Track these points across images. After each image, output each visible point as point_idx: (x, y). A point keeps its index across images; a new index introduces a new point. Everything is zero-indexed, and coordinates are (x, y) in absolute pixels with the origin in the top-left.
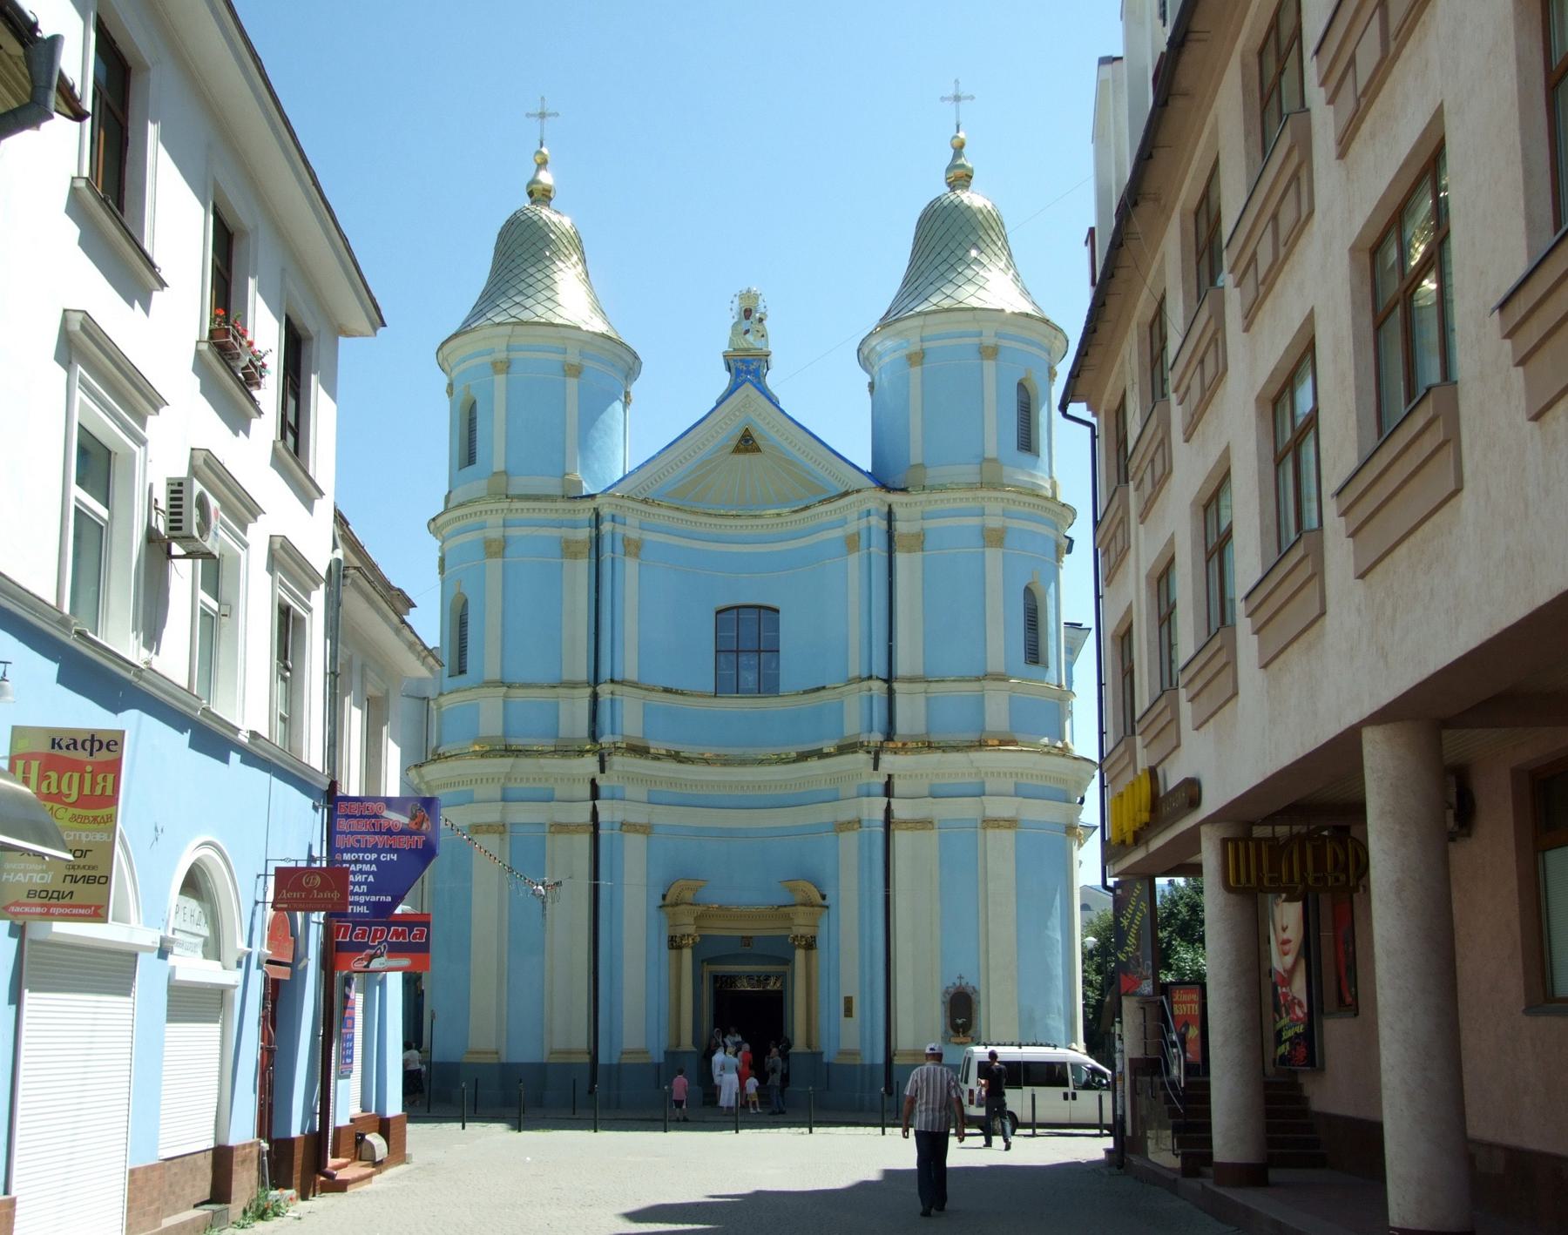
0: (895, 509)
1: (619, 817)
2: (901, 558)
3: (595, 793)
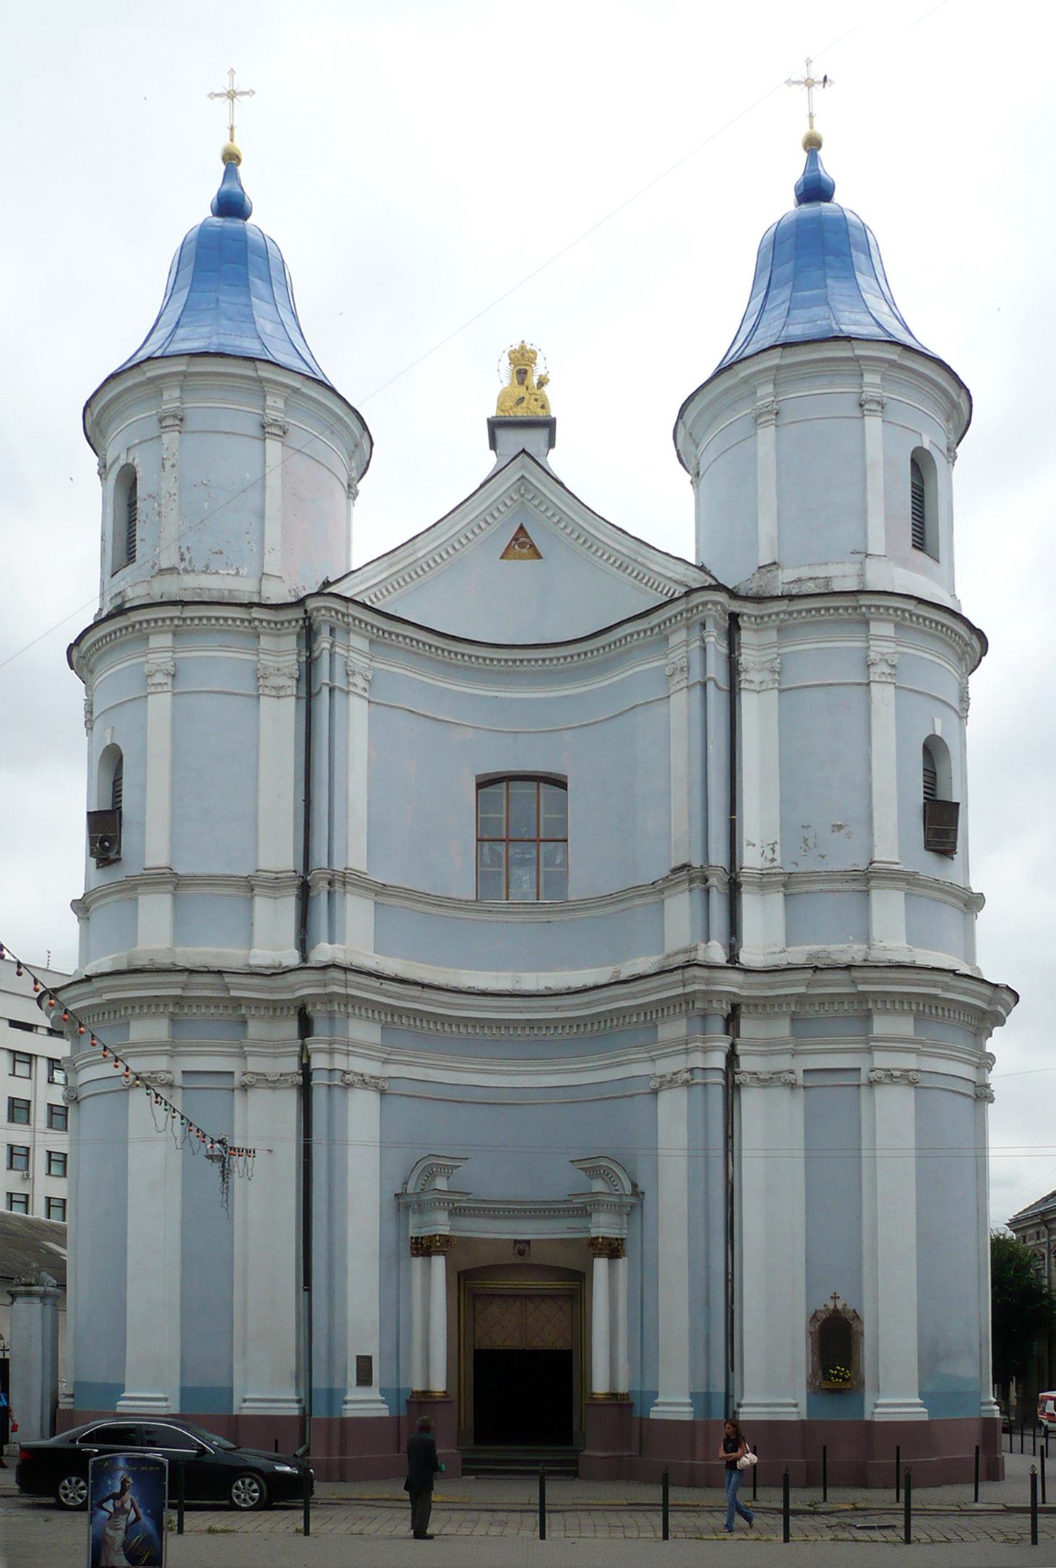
1: (340, 1062)
2: (749, 704)
3: (306, 1027)
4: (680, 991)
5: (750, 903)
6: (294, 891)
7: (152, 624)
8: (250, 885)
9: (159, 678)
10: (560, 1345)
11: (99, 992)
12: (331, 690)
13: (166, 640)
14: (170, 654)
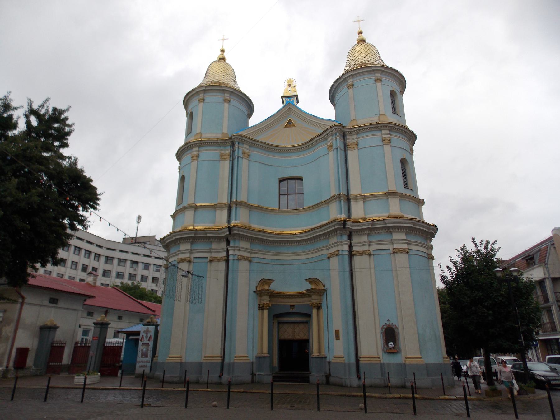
2: (349, 153)
3: (228, 243)
4: (334, 228)
5: (353, 203)
9: (195, 158)
10: (305, 338)
11: (172, 237)
12: (238, 158)
13: (197, 149)
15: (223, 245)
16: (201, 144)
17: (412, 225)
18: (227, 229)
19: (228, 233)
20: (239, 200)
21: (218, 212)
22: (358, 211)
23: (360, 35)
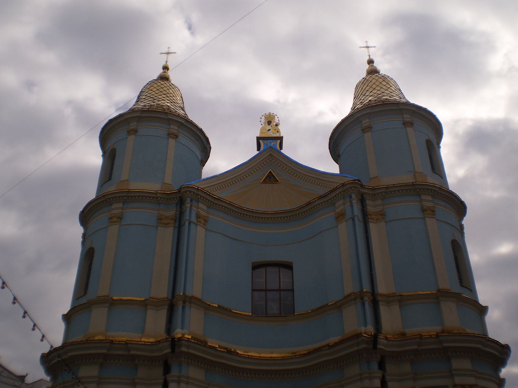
0: (365, 196)
2: (372, 226)
4: (355, 348)
5: (383, 310)
6: (167, 307)
7: (115, 199)
8: (145, 304)
9: (115, 219)
13: (120, 205)
14: (121, 210)
15: (158, 372)
16: (129, 197)
17: (480, 346)
18: (168, 344)
19: (169, 350)
20: (189, 293)
21: (150, 313)
22: (391, 320)
23: (371, 64)
